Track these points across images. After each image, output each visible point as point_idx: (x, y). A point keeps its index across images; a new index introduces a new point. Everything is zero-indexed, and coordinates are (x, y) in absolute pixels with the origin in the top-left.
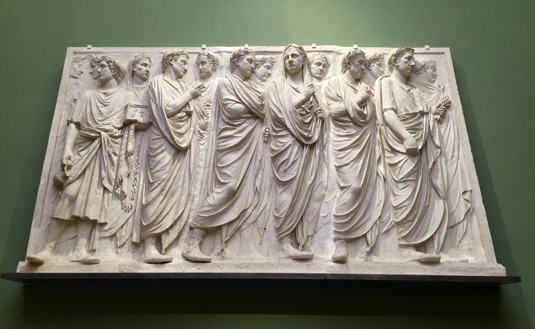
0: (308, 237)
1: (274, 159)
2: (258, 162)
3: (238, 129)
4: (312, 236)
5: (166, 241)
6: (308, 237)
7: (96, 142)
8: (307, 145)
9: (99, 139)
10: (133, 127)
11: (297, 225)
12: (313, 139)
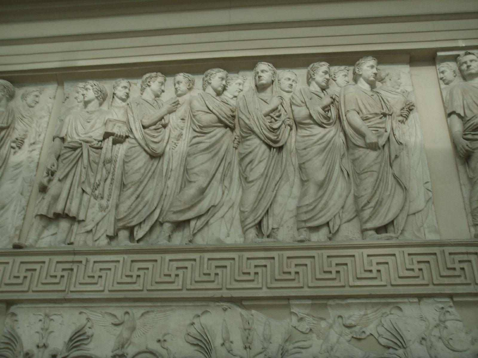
0: (273, 229)
1: (242, 159)
2: (227, 163)
3: (209, 135)
4: (278, 228)
5: (139, 234)
6: (273, 229)
7: (79, 150)
8: (274, 148)
9: (81, 149)
10: (111, 139)
11: (263, 218)
12: (280, 142)
